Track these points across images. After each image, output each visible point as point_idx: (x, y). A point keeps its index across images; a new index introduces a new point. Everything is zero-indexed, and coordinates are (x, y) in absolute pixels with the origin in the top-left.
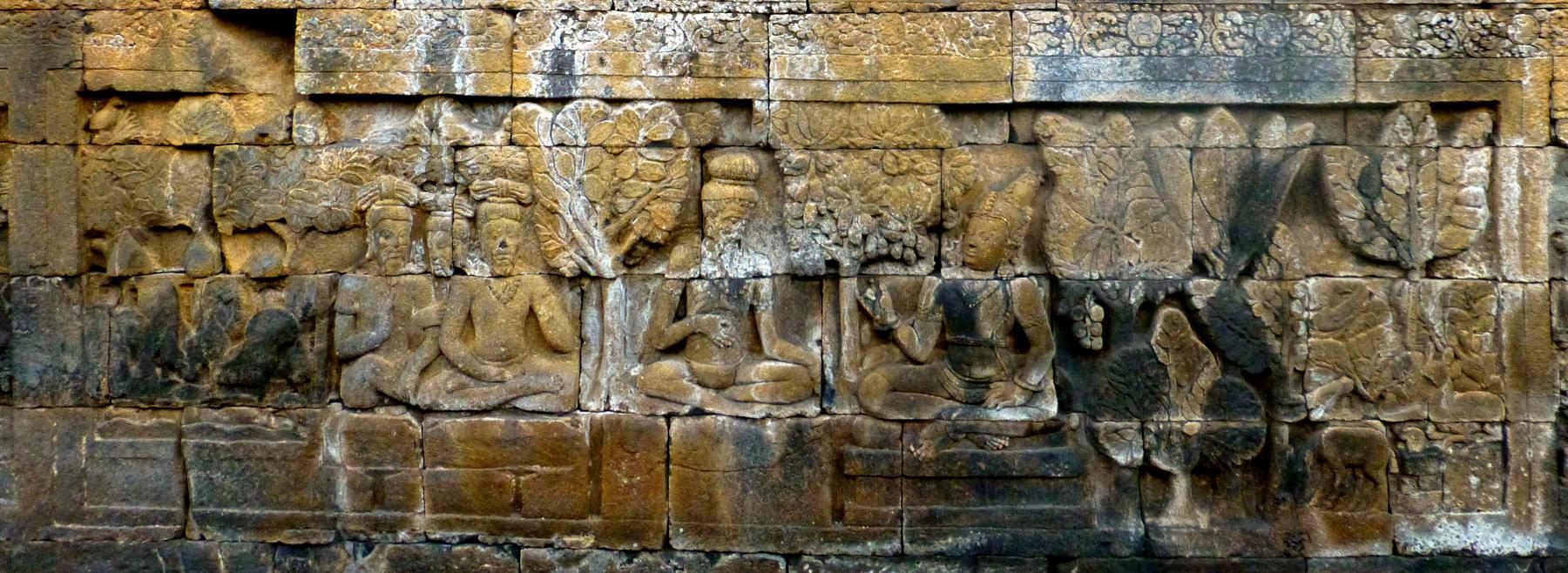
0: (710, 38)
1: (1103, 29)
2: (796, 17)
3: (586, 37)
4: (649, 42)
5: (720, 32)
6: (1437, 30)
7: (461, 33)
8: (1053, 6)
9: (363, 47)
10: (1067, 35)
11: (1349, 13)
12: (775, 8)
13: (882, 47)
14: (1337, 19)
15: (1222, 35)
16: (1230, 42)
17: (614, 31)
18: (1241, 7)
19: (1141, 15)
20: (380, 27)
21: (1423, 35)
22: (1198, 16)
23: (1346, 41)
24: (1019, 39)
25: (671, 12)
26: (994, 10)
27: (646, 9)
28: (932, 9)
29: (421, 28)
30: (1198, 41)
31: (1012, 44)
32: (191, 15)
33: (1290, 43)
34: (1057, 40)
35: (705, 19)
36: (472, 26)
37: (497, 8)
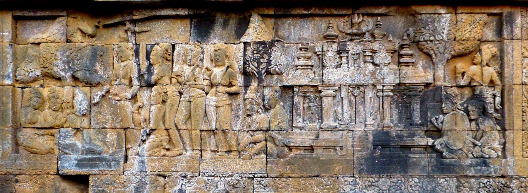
0: (233, 186)
1: (370, 184)
2: (263, 179)
3: (190, 185)
4: (212, 187)
5: (237, 184)
6: (486, 185)
7: (147, 184)
8: (353, 176)
9: (113, 188)
10: (357, 186)
11: (455, 179)
12: (256, 175)
13: (293, 189)
14: (451, 181)
15: (411, 186)
16: (414, 188)
17: (200, 183)
18: (418, 176)
19: (383, 179)
20: (118, 181)
21: (481, 187)
22: (403, 180)
23: (454, 188)
24: (340, 187)
25: (220, 177)
26: (332, 177)
27: (211, 176)
28: (310, 177)
29: (133, 182)
30: (403, 188)
31: (338, 189)
32: (53, 177)
33: (435, 189)
34: (353, 187)
35: (231, 179)
36: (150, 181)
37: (159, 175)
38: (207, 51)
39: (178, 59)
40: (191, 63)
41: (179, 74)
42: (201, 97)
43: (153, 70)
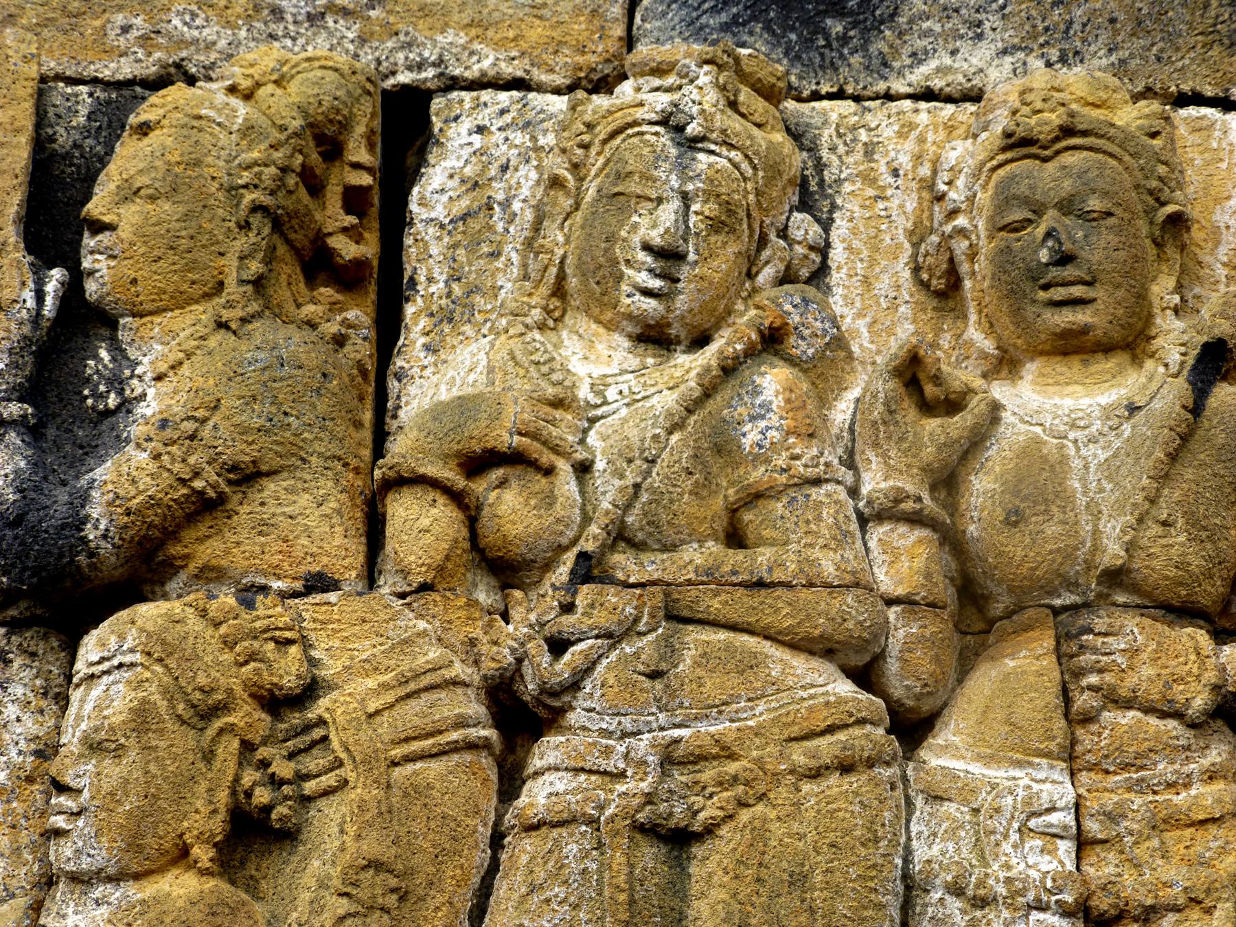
38: (869, 179)
39: (471, 271)
40: (682, 303)
41: (505, 439)
42: (846, 768)
43: (117, 383)
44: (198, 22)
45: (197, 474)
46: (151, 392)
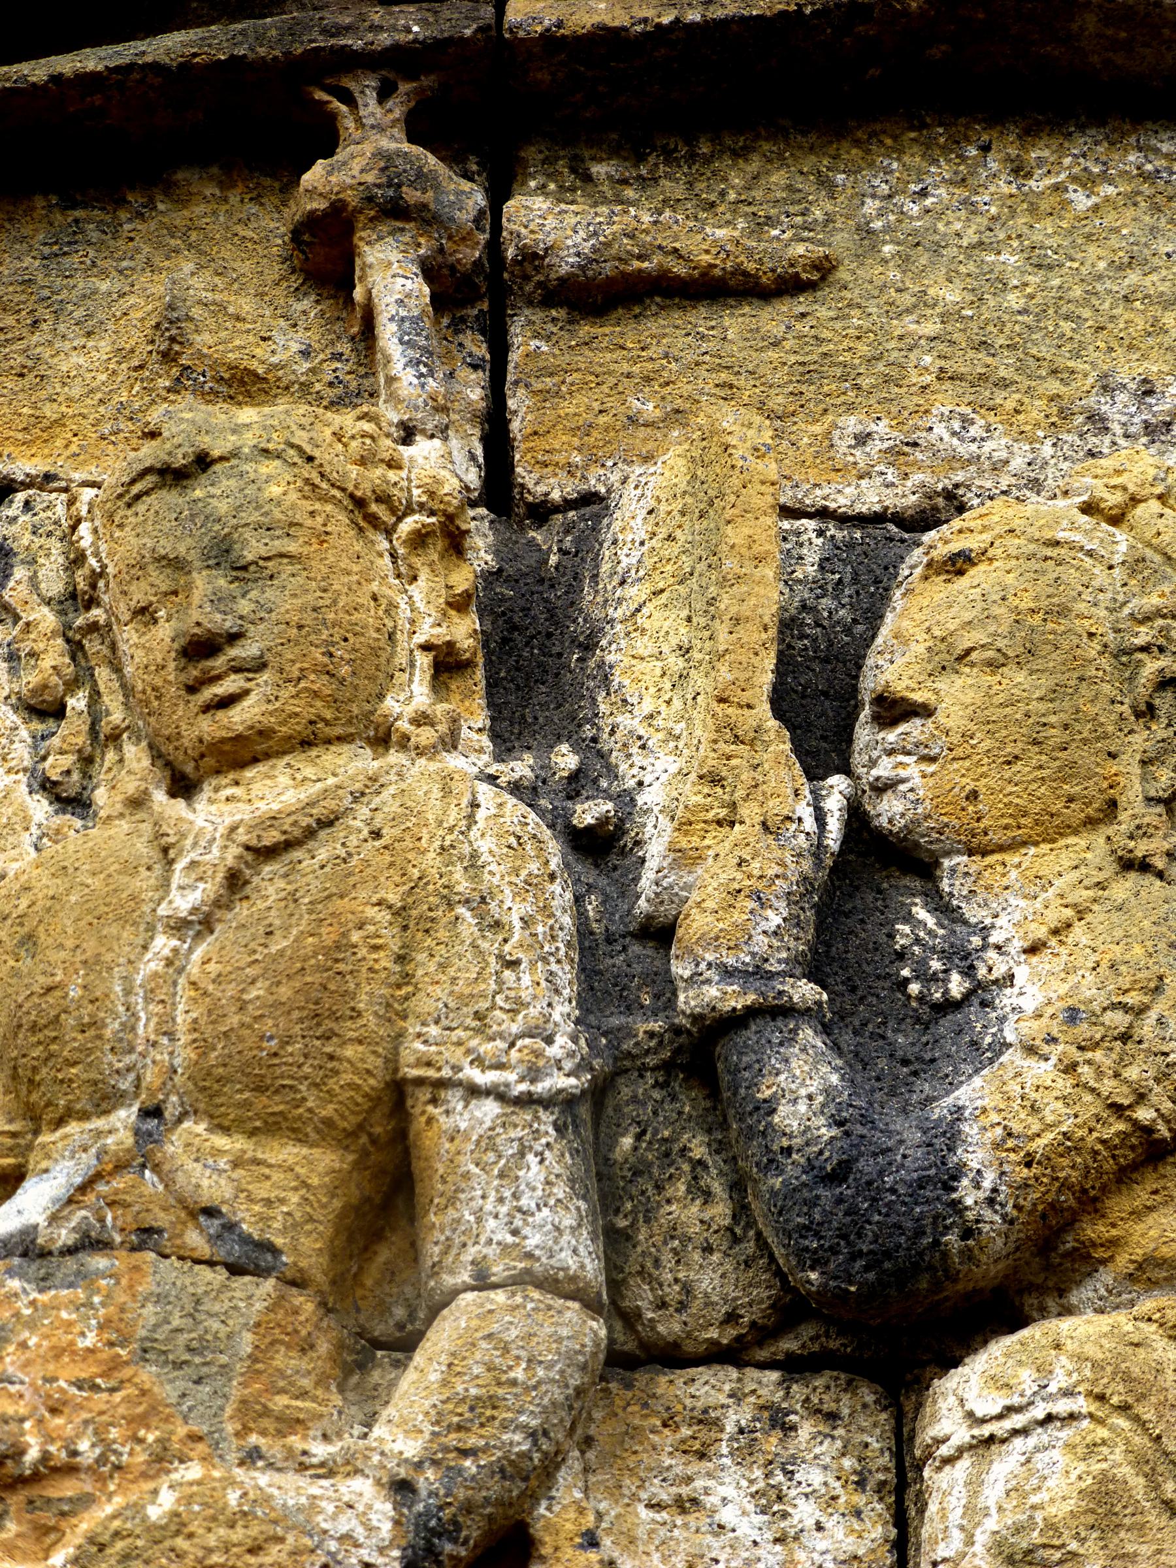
44: (974, 431)
45: (1141, 1097)
46: (1022, 974)
